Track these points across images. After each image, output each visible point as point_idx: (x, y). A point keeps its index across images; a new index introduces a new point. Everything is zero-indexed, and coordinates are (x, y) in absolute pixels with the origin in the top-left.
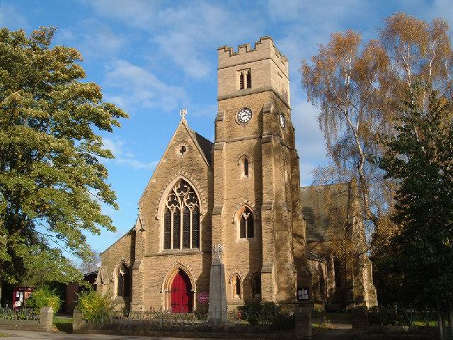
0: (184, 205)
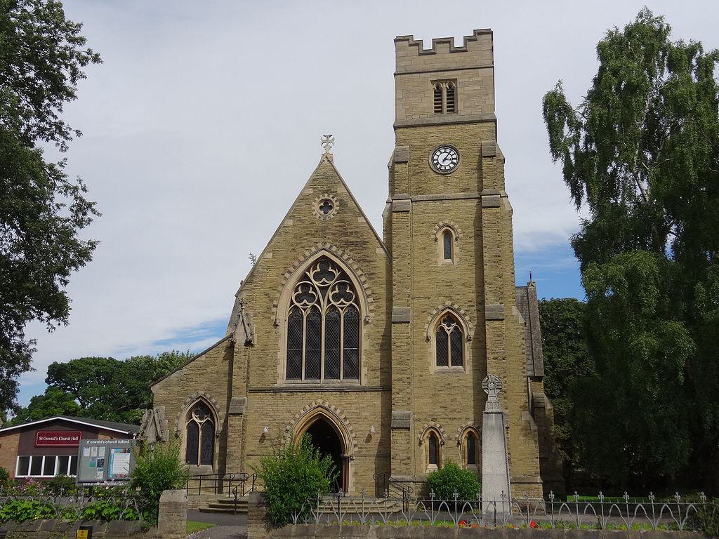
0: (329, 302)
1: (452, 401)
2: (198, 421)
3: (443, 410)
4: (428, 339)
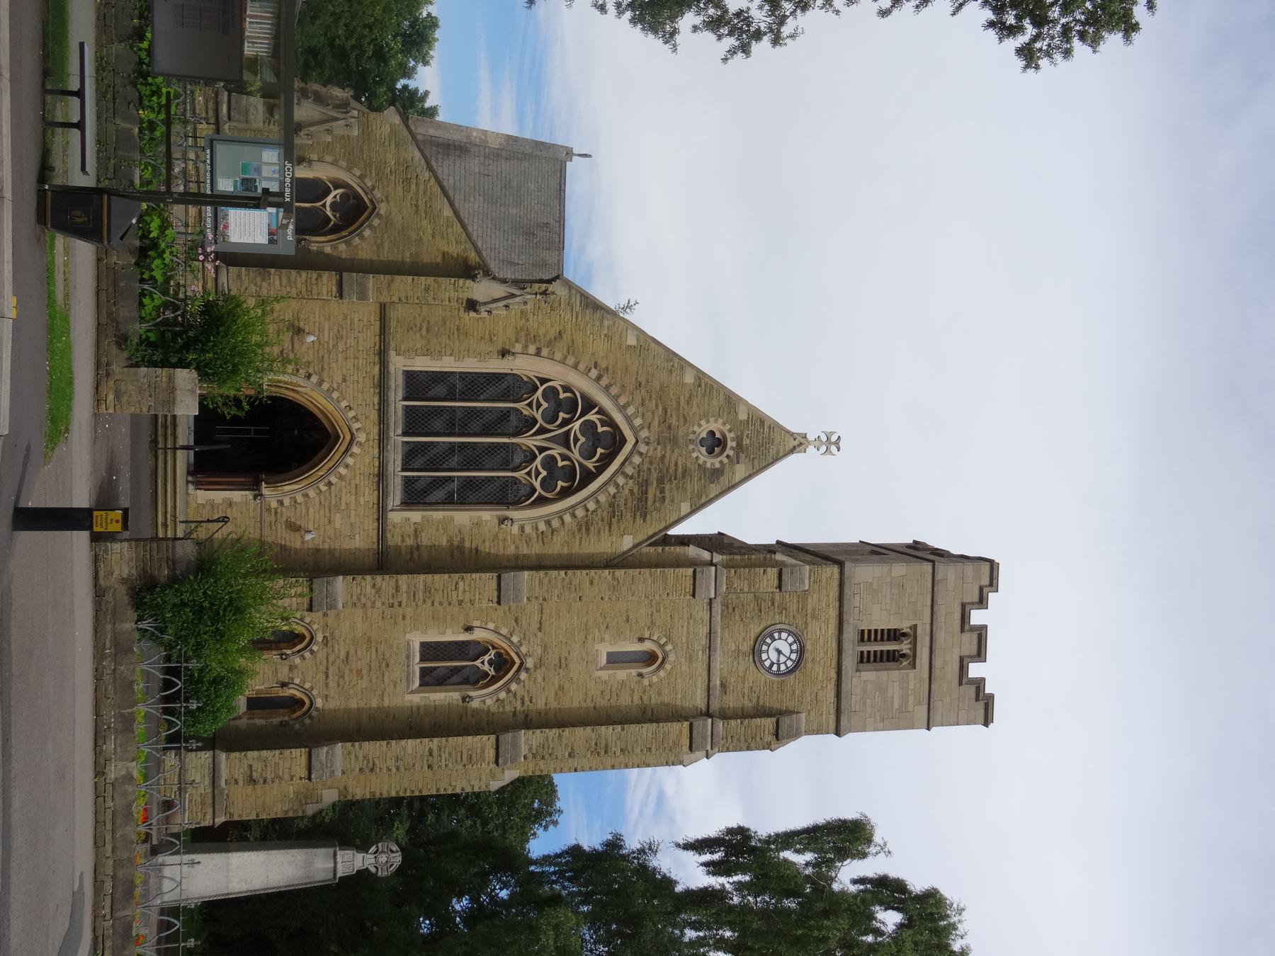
0: (542, 450)
1: (359, 672)
2: (329, 200)
3: (343, 656)
4: (469, 629)
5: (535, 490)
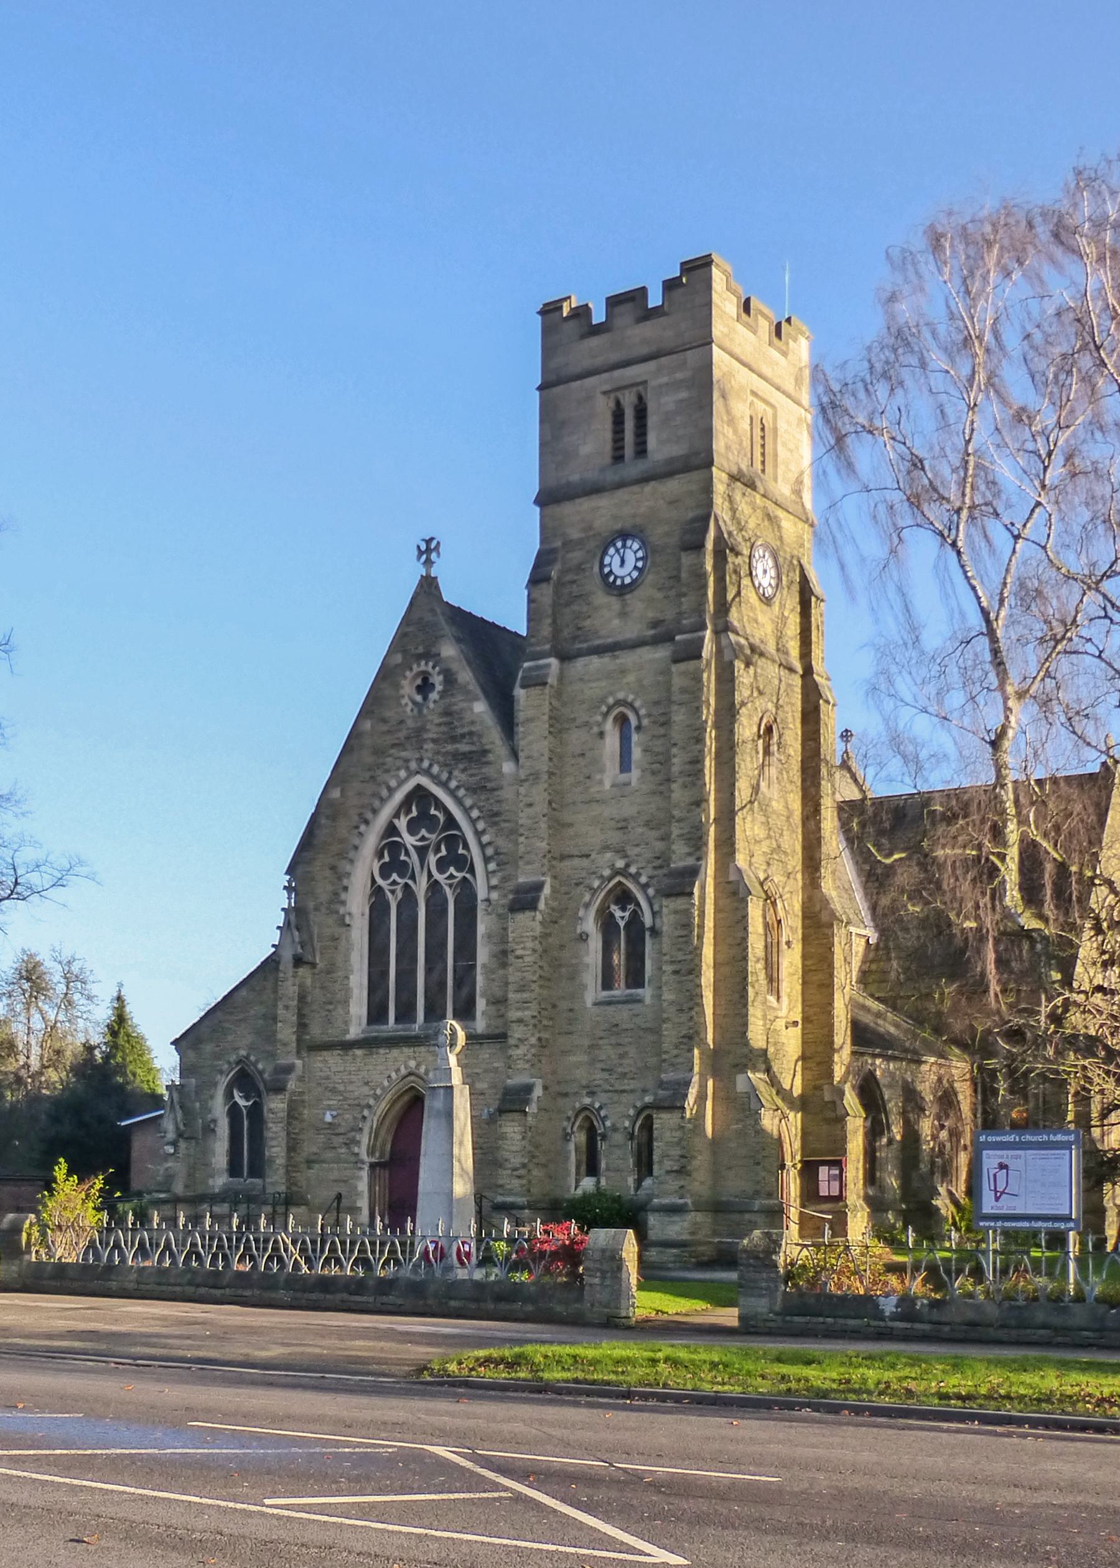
0: (430, 875)
2: (242, 1103)
3: (606, 1075)
4: (584, 938)
5: (464, 878)
